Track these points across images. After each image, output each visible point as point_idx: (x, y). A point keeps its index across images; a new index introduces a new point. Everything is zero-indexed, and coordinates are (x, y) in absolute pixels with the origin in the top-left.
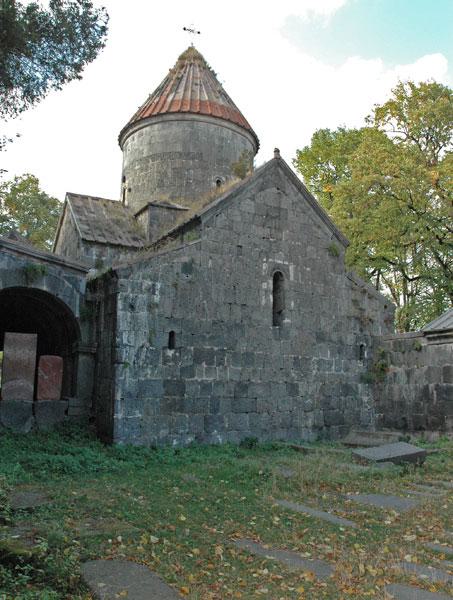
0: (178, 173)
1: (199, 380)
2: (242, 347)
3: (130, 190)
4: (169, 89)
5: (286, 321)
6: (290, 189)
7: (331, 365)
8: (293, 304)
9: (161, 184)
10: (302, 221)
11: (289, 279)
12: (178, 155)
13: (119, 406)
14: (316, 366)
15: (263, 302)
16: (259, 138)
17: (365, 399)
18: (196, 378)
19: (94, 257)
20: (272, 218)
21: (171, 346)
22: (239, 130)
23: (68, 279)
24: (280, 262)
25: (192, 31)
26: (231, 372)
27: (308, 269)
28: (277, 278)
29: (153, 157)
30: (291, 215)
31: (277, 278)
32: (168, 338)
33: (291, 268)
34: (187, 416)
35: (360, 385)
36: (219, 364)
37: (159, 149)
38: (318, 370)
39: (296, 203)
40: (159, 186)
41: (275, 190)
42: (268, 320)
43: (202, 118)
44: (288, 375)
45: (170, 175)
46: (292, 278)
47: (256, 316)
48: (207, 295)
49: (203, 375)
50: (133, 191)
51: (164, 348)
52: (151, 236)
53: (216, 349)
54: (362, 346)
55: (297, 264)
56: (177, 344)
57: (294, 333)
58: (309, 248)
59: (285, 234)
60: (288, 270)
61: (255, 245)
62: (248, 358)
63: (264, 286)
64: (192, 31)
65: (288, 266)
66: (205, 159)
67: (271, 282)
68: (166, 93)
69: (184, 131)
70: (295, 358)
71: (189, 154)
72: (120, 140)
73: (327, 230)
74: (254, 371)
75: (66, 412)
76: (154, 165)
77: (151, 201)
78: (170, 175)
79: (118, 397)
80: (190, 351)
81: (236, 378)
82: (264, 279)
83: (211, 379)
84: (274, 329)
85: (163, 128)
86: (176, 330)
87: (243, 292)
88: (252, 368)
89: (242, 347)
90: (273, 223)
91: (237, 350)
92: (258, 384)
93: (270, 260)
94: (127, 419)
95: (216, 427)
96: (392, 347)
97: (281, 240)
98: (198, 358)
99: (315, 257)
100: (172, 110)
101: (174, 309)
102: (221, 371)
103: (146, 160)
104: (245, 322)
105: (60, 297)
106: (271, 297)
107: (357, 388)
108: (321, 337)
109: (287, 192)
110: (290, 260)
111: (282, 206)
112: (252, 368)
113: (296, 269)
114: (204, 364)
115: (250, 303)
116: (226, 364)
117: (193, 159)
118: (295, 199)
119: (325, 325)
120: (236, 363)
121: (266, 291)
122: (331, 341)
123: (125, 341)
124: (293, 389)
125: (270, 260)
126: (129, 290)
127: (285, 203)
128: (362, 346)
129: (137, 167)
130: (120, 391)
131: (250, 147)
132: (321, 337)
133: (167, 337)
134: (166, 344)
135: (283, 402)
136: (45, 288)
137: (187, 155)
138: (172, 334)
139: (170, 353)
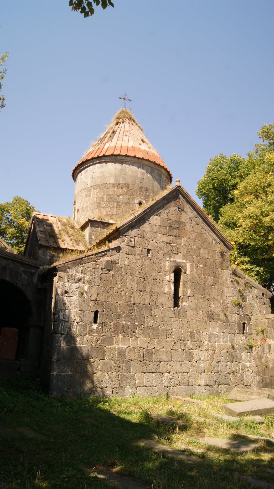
0: (111, 198)
2: (150, 323)
3: (78, 211)
4: (106, 139)
6: (188, 208)
8: (189, 291)
9: (99, 206)
10: (197, 231)
11: (185, 273)
12: (112, 186)
13: (55, 366)
15: (166, 290)
16: (171, 173)
17: (248, 365)
18: (114, 346)
19: (48, 257)
20: (174, 229)
21: (95, 321)
22: (156, 167)
23: (24, 272)
25: (126, 99)
26: (141, 341)
27: (201, 266)
28: (178, 272)
29: (95, 187)
30: (188, 227)
31: (178, 272)
32: (93, 315)
33: (188, 265)
37: (98, 182)
38: (209, 341)
39: (193, 218)
40: (98, 208)
41: (176, 208)
43: (129, 159)
45: (105, 200)
46: (188, 272)
47: (160, 300)
48: (123, 283)
49: (120, 343)
50: (80, 211)
51: (90, 323)
52: (90, 243)
55: (192, 262)
56: (98, 321)
57: (190, 313)
58: (202, 251)
59: (183, 241)
61: (161, 249)
62: (155, 330)
63: (167, 278)
64: (126, 99)
65: (185, 264)
66: (131, 187)
67: (172, 275)
68: (105, 142)
69: (116, 169)
71: (119, 184)
72: (73, 176)
73: (216, 238)
75: (19, 370)
76: (95, 193)
77: (91, 218)
78: (105, 200)
79: (55, 359)
85: (102, 167)
86: (100, 310)
87: (150, 282)
89: (150, 323)
90: (175, 232)
91: (146, 325)
93: (172, 259)
94: (60, 375)
95: (129, 383)
96: (267, 324)
97: (180, 244)
98: (116, 332)
100: (106, 154)
101: (98, 294)
102: (133, 340)
103: (90, 189)
104: (152, 304)
105: (19, 285)
107: (241, 356)
108: (211, 316)
109: (185, 210)
110: (187, 259)
111: (182, 220)
113: (192, 267)
114: (120, 336)
115: (156, 290)
116: (137, 335)
117: (122, 188)
118: (192, 215)
119: (215, 307)
120: (145, 335)
121: (169, 281)
122: (219, 319)
123: (61, 318)
125: (172, 259)
126: (66, 280)
127: (184, 218)
128: (244, 324)
129: (83, 194)
130: (56, 354)
131: (164, 178)
132: (211, 316)
133: (93, 315)
134: (92, 320)
136: (8, 279)
137: (118, 185)
138: (96, 313)
139: (95, 326)
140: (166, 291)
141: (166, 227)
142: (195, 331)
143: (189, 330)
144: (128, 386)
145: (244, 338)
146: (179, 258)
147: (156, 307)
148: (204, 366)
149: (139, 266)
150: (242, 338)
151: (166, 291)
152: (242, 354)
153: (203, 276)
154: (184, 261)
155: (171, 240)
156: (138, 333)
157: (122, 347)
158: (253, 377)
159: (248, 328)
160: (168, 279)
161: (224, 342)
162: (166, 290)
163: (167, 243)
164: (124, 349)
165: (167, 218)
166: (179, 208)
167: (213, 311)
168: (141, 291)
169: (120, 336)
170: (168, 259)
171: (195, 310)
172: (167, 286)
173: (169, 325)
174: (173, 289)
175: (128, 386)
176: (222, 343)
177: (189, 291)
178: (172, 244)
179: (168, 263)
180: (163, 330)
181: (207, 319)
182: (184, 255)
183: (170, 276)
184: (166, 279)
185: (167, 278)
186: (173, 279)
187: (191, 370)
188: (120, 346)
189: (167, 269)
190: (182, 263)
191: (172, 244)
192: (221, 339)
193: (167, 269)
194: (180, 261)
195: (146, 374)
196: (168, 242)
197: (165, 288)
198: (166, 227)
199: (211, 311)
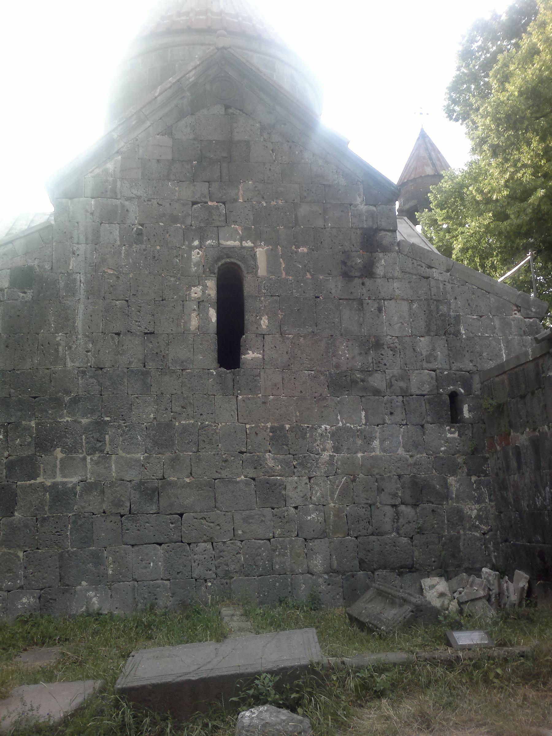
1: (48, 483)
5: (250, 356)
7: (373, 438)
8: (264, 322)
14: (329, 444)
15: (194, 323)
17: (472, 510)
18: (39, 480)
24: (230, 243)
27: (303, 250)
33: (261, 253)
34: (21, 554)
35: (451, 480)
36: (93, 450)
38: (337, 450)
42: (206, 356)
44: (258, 464)
46: (262, 271)
53: (84, 421)
54: (453, 396)
60: (254, 257)
61: (174, 219)
63: (196, 292)
65: (252, 249)
67: (211, 284)
70: (273, 430)
74: (175, 460)
80: (29, 428)
81: (133, 475)
82: (199, 281)
83: (75, 480)
84: (219, 375)
88: (168, 455)
92: (185, 486)
93: (209, 242)
97: (235, 200)
99: (320, 223)
104: (151, 366)
106: (213, 315)
107: (446, 485)
110: (257, 237)
112: (168, 455)
113: (272, 258)
114: (59, 454)
116: (108, 448)
121: (200, 302)
124: (269, 491)
128: (453, 396)
135: (245, 520)
140: (192, 328)
141: (191, 161)
142: (287, 427)
143: (269, 425)
144: (84, 583)
145: (456, 435)
146: (231, 238)
147: (164, 371)
148: (321, 519)
149: (111, 272)
150: (449, 435)
151: (192, 328)
152: (451, 480)
153: (308, 276)
154: (249, 244)
155: (206, 191)
156: (111, 441)
157: (64, 483)
158: (491, 546)
159: (466, 408)
160: (200, 294)
161: (384, 450)
162: (194, 323)
163: (194, 203)
164: (70, 485)
165: (192, 136)
166: (227, 107)
167: (344, 368)
168: (118, 334)
169: (59, 454)
170: (196, 243)
171: (287, 367)
172: (194, 315)
173: (204, 417)
174: (214, 319)
175: (84, 583)
176: (378, 452)
177: (264, 322)
178: (210, 203)
179: (196, 255)
180: (185, 429)
181: (325, 391)
182: (246, 229)
183: (205, 287)
184: (193, 295)
185: (196, 292)
186: (212, 292)
187: (278, 532)
188: (59, 479)
189: (194, 269)
190: (242, 247)
191: (210, 203)
192: (376, 443)
193: (194, 269)
194: (237, 243)
195: (136, 548)
196: (196, 198)
197: (190, 320)
198: (191, 161)
199: (337, 366)
